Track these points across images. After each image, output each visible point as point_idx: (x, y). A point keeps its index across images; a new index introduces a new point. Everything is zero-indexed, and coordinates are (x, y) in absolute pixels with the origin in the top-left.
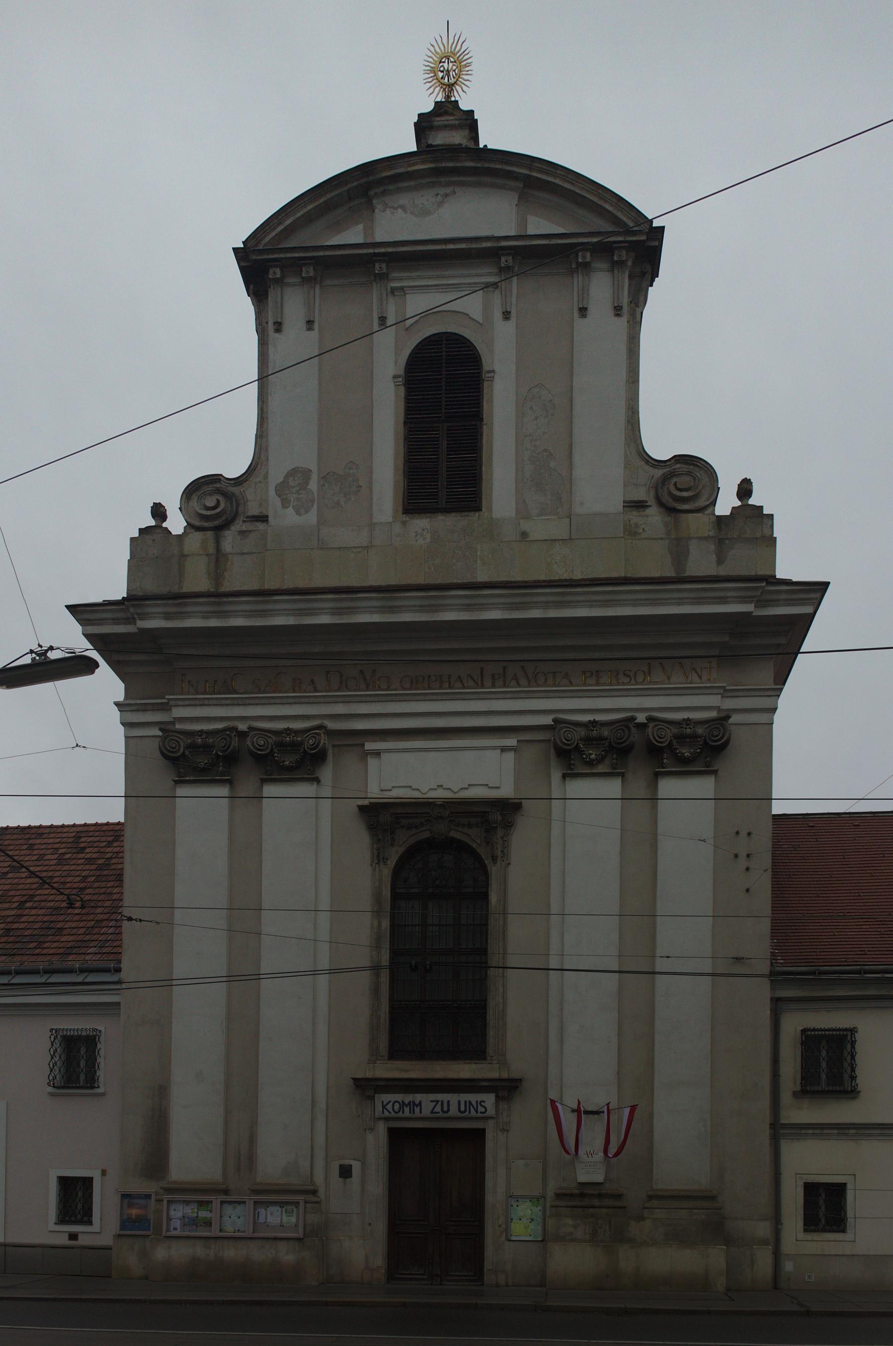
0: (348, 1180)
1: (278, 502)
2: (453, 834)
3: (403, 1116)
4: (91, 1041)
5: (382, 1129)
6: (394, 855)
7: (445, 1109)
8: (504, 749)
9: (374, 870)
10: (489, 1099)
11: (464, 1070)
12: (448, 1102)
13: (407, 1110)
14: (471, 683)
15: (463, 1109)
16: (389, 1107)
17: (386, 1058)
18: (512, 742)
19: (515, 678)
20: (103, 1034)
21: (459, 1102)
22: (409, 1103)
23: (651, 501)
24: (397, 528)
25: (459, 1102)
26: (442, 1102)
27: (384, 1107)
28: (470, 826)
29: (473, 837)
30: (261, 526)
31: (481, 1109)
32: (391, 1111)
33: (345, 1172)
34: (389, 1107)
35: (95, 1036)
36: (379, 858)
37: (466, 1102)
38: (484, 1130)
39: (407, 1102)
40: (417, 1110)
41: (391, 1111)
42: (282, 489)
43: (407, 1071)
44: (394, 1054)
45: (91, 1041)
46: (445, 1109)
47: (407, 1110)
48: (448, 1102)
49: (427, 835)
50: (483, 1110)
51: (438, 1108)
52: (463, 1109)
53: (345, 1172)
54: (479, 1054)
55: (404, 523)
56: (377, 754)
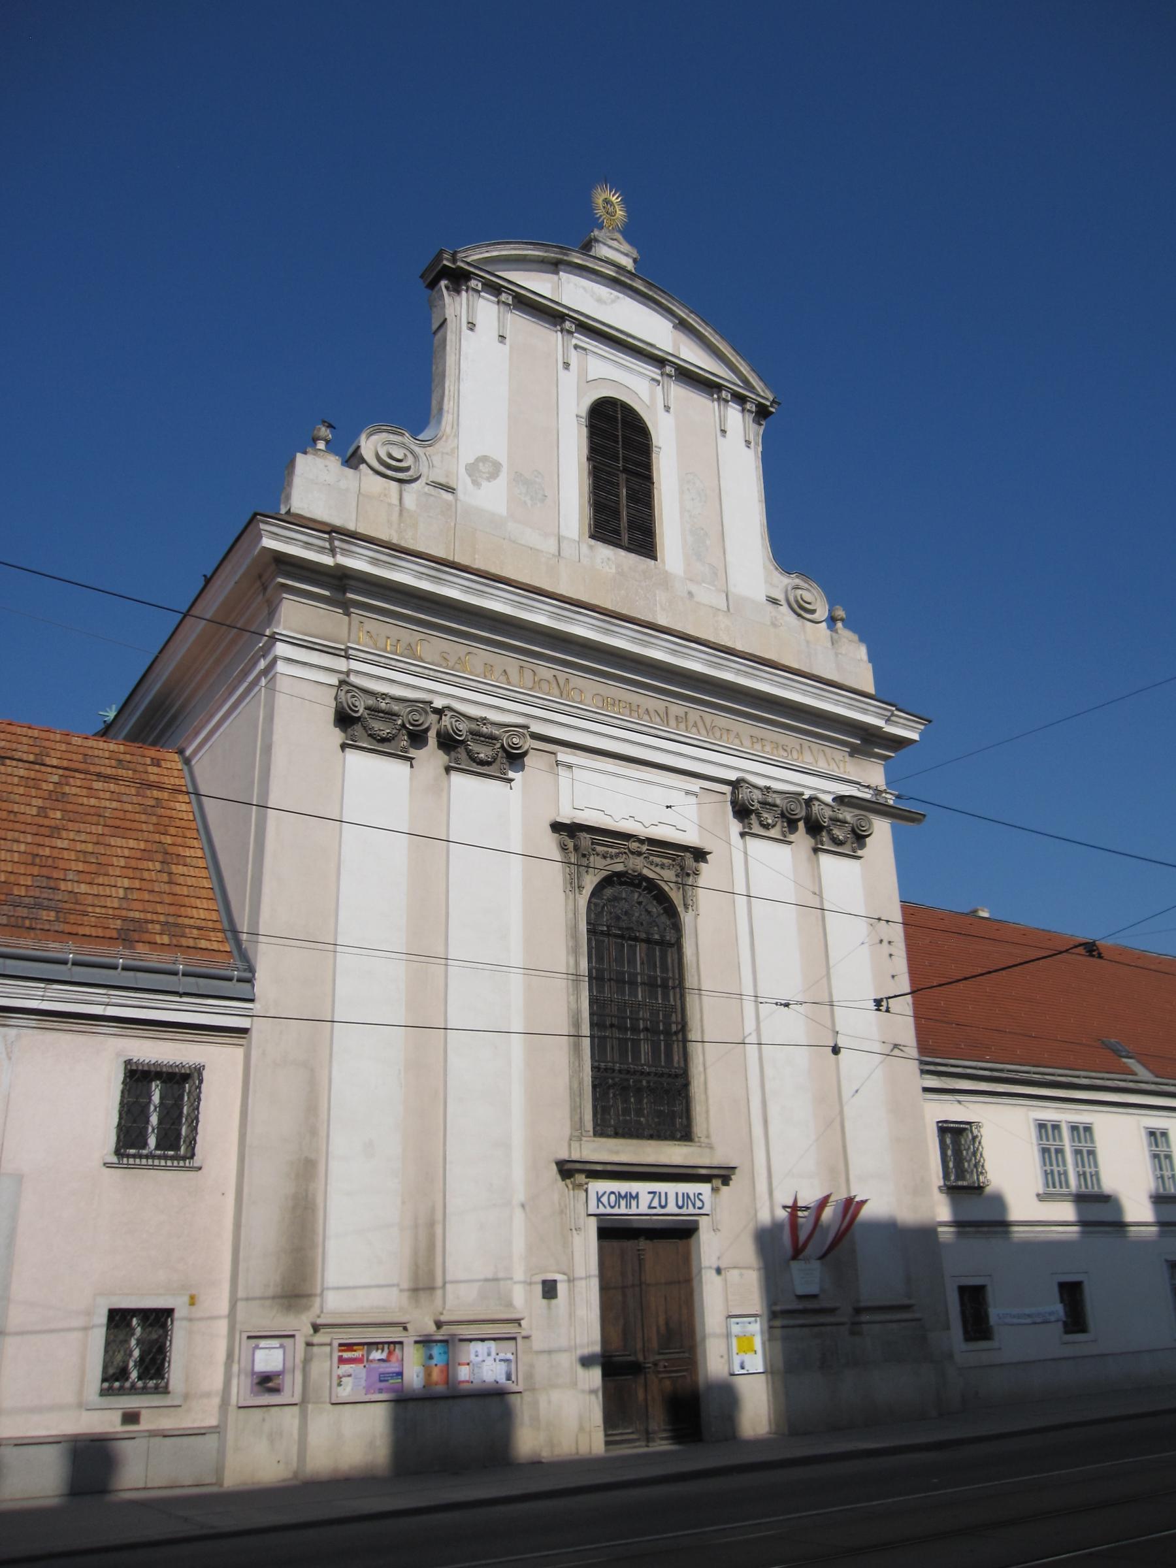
0: (554, 1301)
1: (468, 480)
2: (645, 872)
4: (181, 1082)
5: (592, 1226)
6: (590, 882)
7: (663, 1203)
8: (688, 793)
9: (567, 897)
10: (705, 1188)
11: (673, 1154)
13: (623, 1203)
14: (658, 719)
15: (680, 1203)
16: (604, 1199)
17: (591, 1133)
18: (695, 785)
19: (695, 725)
22: (626, 1196)
23: (783, 602)
24: (584, 549)
27: (599, 1200)
29: (665, 876)
30: (448, 497)
31: (699, 1204)
32: (606, 1203)
33: (549, 1290)
36: (574, 885)
39: (623, 1194)
40: (634, 1203)
41: (606, 1203)
42: (472, 469)
43: (617, 1153)
44: (603, 1128)
45: (181, 1082)
46: (663, 1203)
47: (623, 1203)
49: (619, 868)
51: (655, 1203)
52: (680, 1203)
53: (549, 1290)
54: (685, 1134)
55: (591, 547)
56: (570, 767)
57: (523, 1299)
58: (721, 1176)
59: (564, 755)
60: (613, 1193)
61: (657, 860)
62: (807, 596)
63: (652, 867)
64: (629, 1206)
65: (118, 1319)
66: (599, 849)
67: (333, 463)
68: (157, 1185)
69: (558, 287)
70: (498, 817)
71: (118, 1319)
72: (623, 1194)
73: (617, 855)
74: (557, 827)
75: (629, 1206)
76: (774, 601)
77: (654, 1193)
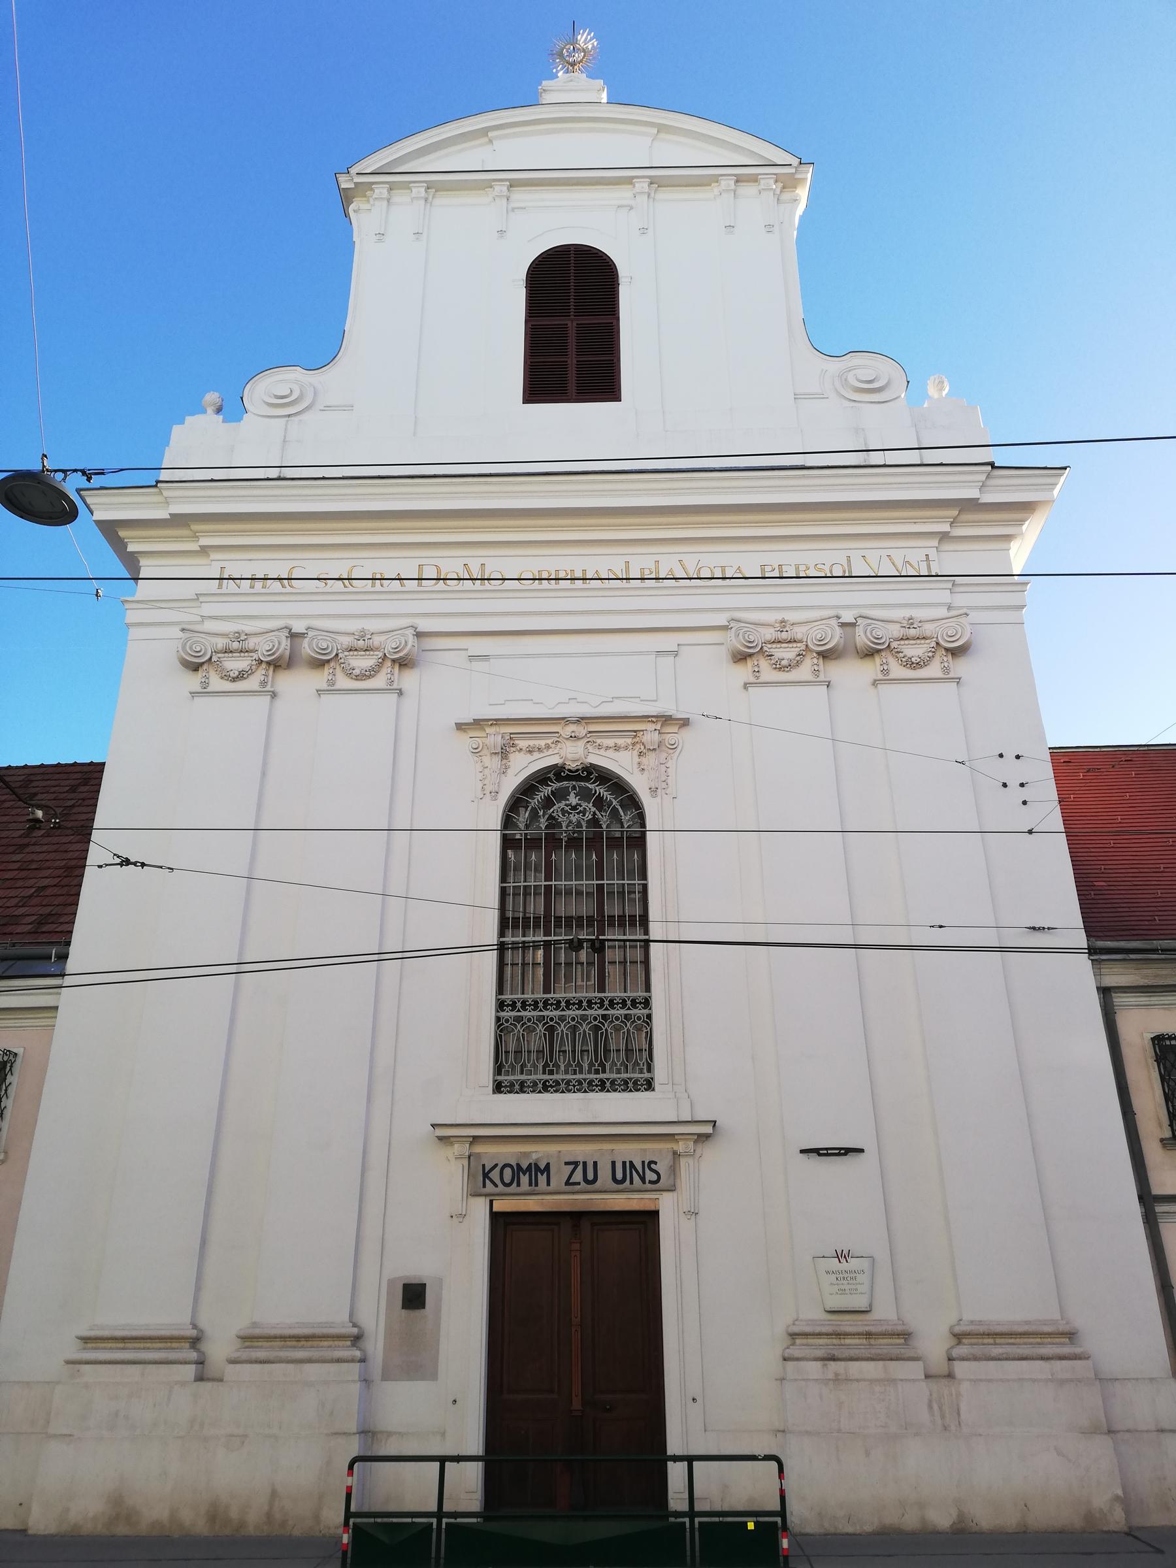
3: (519, 1190)
7: (590, 1177)
12: (595, 1163)
13: (525, 1179)
15: (619, 1176)
16: (495, 1175)
18: (668, 642)
20: (19, 1060)
21: (613, 1163)
25: (613, 1163)
26: (585, 1163)
27: (486, 1175)
28: (617, 748)
32: (498, 1181)
34: (495, 1175)
35: (5, 1063)
37: (624, 1163)
38: (654, 1214)
39: (524, 1166)
40: (542, 1179)
41: (498, 1181)
46: (590, 1177)
47: (525, 1179)
48: (595, 1163)
50: (655, 1177)
51: (578, 1176)
52: (619, 1176)
60: (510, 1166)
61: (610, 742)
63: (602, 752)
64: (534, 1182)
66: (522, 744)
72: (524, 1166)
73: (548, 747)
75: (534, 1182)
77: (576, 1164)
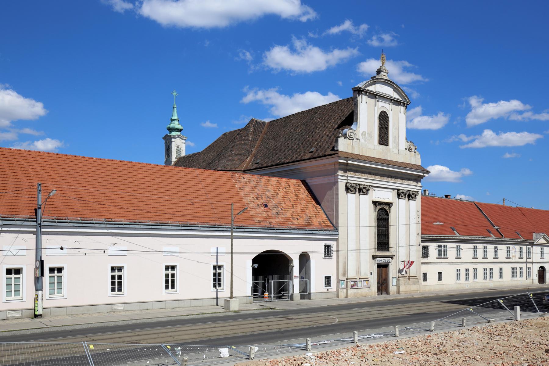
18: (392, 190)
29: (387, 208)
33: (371, 274)
42: (362, 134)
53: (371, 274)
54: (388, 250)
57: (369, 275)
58: (392, 257)
59: (374, 189)
62: (411, 147)
65: (325, 277)
67: (343, 138)
68: (328, 260)
69: (375, 88)
70: (366, 201)
71: (325, 277)
74: (373, 202)
76: (406, 149)
